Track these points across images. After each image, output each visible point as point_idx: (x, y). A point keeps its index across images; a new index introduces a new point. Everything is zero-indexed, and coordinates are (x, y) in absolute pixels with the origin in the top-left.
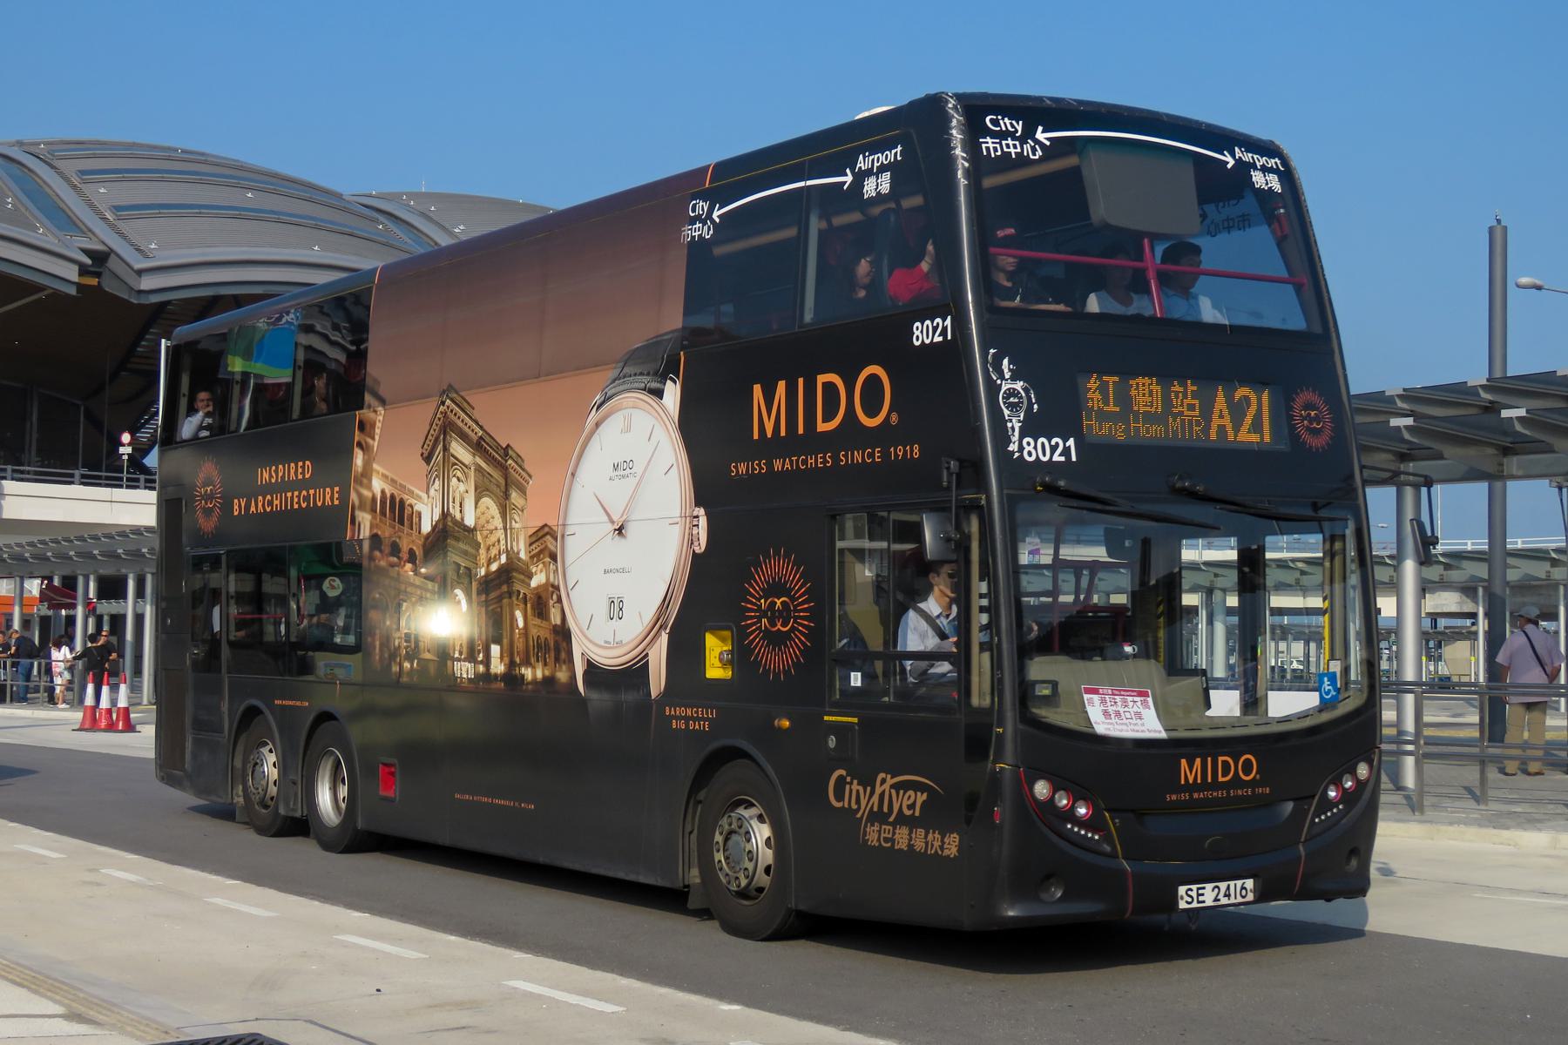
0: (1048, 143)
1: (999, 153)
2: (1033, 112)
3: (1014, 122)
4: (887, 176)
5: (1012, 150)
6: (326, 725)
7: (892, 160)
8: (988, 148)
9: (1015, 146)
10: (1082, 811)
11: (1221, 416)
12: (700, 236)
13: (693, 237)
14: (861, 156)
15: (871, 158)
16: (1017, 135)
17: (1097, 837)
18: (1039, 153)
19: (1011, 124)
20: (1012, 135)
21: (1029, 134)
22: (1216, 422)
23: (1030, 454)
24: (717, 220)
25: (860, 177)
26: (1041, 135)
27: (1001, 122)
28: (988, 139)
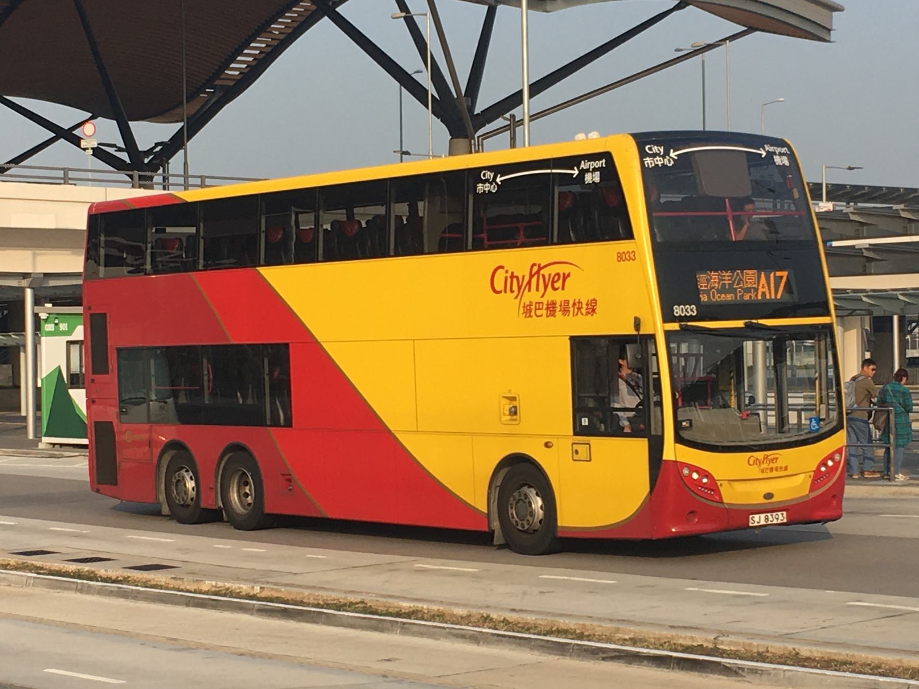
0: (676, 158)
1: (653, 165)
2: (670, 139)
3: (659, 147)
4: (598, 173)
5: (659, 163)
7: (600, 166)
8: (648, 163)
9: (660, 160)
10: (705, 480)
11: (763, 287)
12: (489, 191)
13: (485, 191)
14: (583, 162)
15: (589, 163)
16: (661, 154)
17: (712, 493)
18: (672, 162)
19: (659, 150)
20: (658, 155)
21: (667, 153)
22: (761, 290)
23: (677, 313)
24: (500, 183)
25: (583, 172)
26: (673, 154)
27: (653, 149)
28: (648, 159)
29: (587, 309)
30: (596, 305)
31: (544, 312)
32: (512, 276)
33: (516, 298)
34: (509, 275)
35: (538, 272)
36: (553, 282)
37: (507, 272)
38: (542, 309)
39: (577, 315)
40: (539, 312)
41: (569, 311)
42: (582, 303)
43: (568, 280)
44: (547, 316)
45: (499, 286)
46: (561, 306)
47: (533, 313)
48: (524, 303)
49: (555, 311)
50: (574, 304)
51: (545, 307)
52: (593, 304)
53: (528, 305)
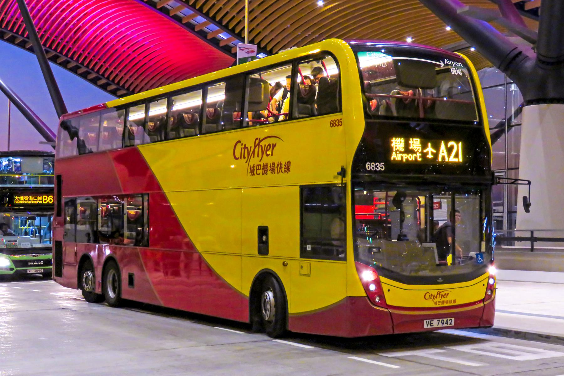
6: (110, 263)
29: (285, 168)
30: (290, 166)
31: (260, 171)
32: (245, 147)
33: (246, 162)
34: (243, 146)
35: (258, 144)
36: (267, 150)
37: (242, 145)
38: (260, 169)
39: (279, 173)
40: (258, 172)
41: (275, 170)
42: (282, 164)
43: (275, 148)
44: (263, 175)
45: (238, 155)
46: (270, 167)
47: (255, 172)
48: (251, 166)
49: (267, 170)
50: (278, 165)
51: (262, 168)
52: (288, 165)
53: (252, 167)
